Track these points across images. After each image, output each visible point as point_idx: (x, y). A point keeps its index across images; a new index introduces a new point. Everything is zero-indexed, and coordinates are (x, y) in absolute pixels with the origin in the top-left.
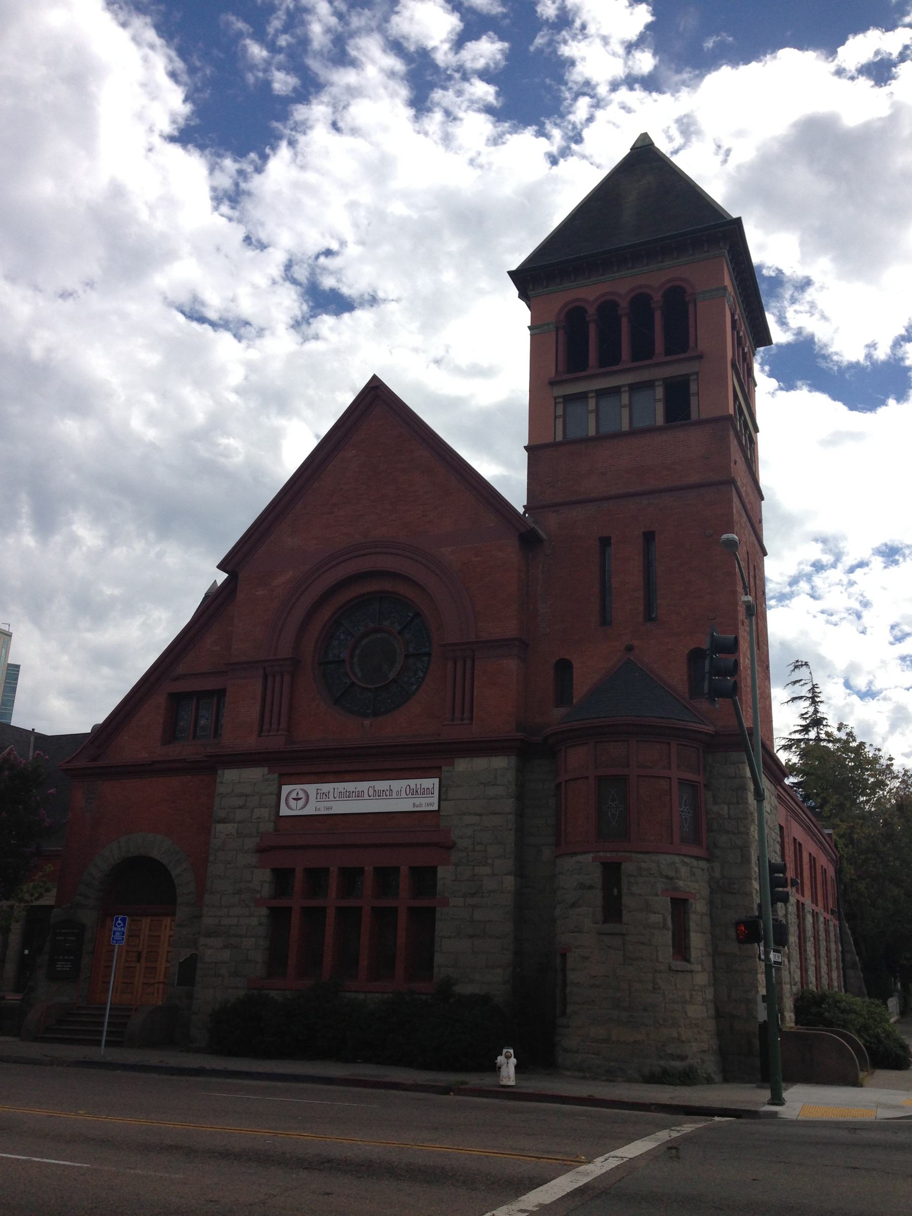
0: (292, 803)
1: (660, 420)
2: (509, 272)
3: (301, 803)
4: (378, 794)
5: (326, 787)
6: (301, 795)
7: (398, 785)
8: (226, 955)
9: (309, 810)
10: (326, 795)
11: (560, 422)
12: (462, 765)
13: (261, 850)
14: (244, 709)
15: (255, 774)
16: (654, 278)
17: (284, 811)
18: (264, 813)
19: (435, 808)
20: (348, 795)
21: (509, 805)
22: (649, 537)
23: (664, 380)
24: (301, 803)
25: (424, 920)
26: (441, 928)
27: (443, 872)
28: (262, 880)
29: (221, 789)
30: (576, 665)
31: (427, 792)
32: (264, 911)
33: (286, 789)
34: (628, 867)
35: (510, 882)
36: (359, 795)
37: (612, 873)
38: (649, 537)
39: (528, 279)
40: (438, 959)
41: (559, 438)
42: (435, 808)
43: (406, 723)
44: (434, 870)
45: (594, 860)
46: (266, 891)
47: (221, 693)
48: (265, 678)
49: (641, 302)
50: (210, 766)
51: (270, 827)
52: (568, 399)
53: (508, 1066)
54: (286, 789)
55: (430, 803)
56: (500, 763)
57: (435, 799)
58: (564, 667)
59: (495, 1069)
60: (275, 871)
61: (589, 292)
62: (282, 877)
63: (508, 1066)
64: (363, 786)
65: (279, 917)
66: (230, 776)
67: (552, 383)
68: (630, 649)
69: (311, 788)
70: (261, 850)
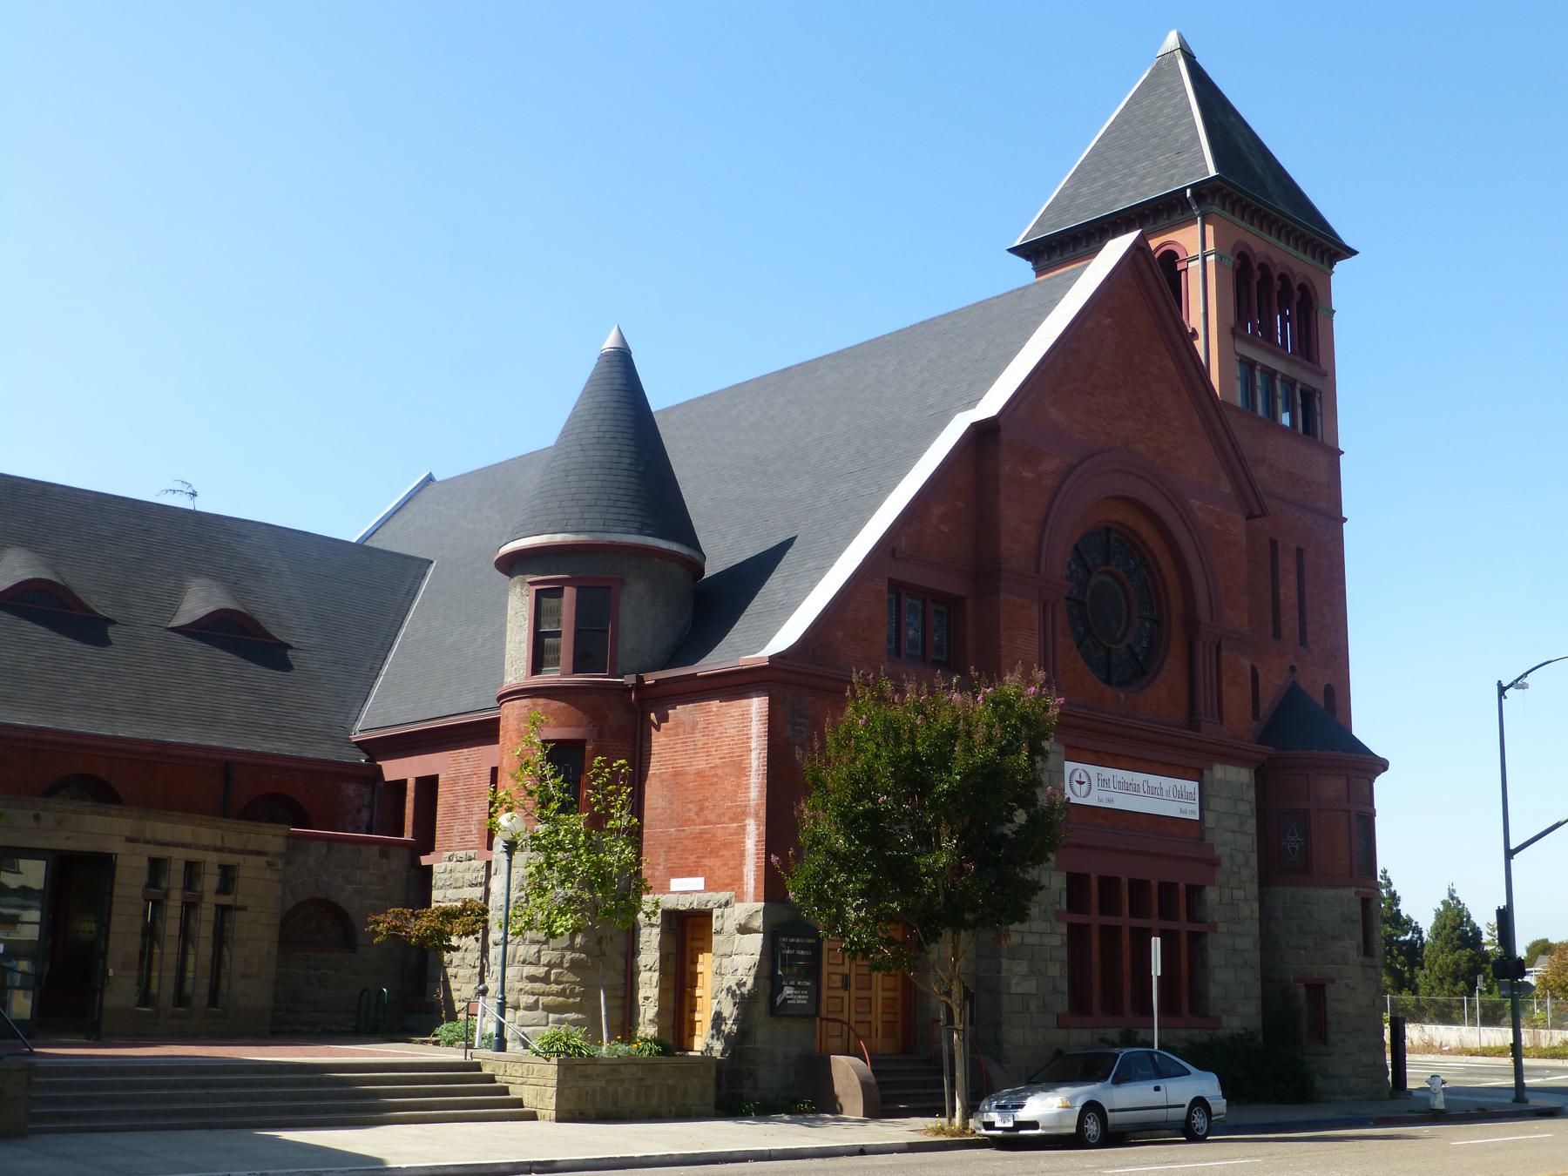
0: (1076, 786)
3: (1085, 787)
4: (1153, 792)
5: (1108, 773)
6: (1084, 779)
7: (1167, 783)
10: (1106, 782)
21: (1251, 825)
24: (1085, 787)
26: (1215, 957)
27: (1211, 894)
31: (1189, 796)
32: (1064, 929)
44: (1201, 888)
45: (1357, 893)
55: (1191, 811)
64: (1139, 778)
65: (1077, 935)
69: (1093, 770)
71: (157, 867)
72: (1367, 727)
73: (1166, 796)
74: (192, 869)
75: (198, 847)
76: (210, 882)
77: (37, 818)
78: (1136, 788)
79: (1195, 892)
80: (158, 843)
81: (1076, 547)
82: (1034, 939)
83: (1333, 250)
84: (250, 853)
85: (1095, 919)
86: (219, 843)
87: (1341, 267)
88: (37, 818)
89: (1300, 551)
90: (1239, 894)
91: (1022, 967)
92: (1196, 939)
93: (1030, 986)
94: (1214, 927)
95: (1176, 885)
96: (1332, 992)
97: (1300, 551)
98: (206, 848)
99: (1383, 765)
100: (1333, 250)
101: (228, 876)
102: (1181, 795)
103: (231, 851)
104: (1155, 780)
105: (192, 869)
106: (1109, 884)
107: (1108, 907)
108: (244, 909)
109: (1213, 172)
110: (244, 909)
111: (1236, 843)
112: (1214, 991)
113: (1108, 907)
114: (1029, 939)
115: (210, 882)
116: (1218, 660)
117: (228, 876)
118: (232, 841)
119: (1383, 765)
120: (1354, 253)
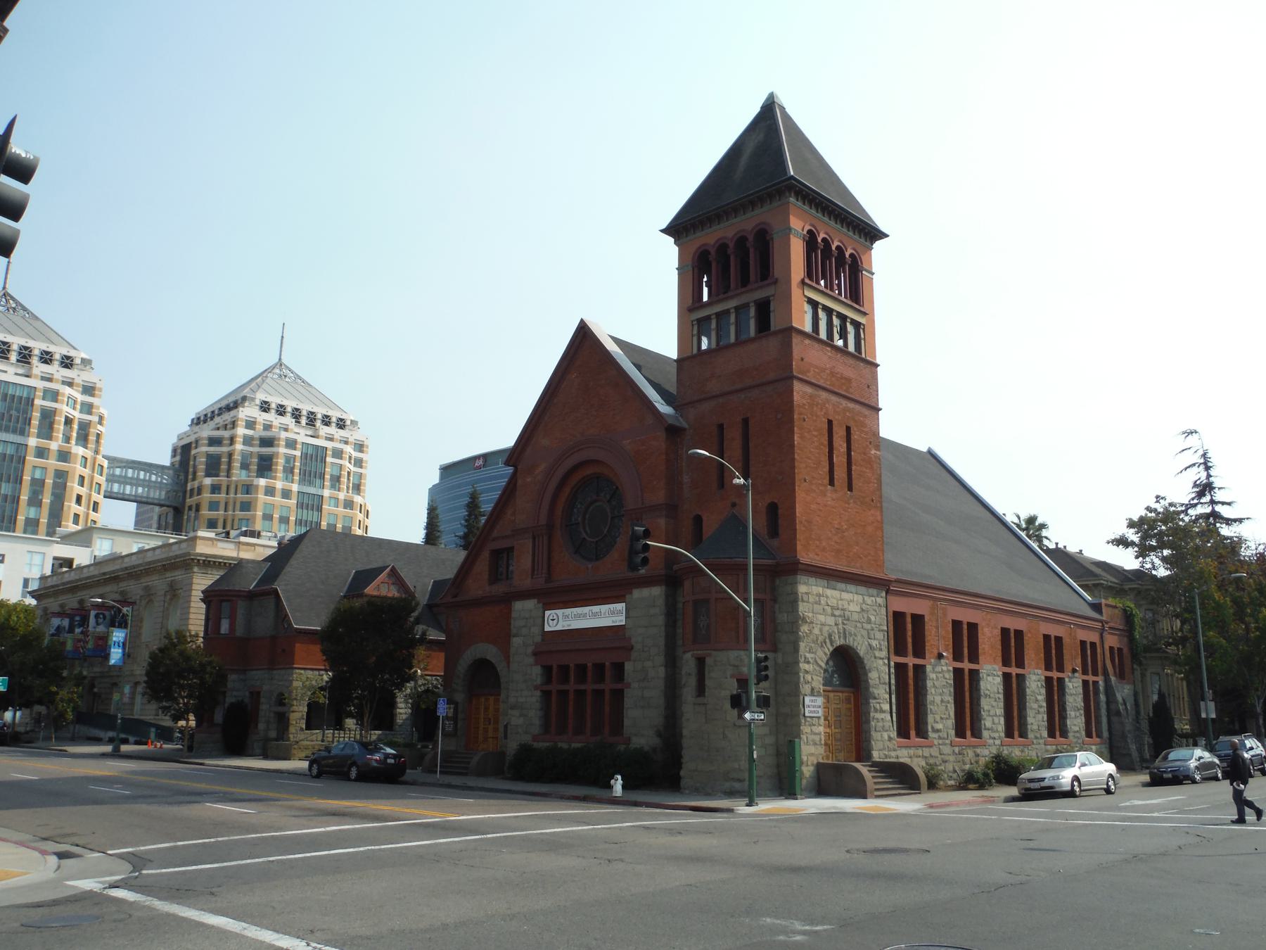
1: (752, 333)
2: (662, 231)
4: (595, 615)
5: (568, 611)
7: (604, 608)
8: (521, 721)
9: (559, 628)
11: (695, 339)
12: (637, 593)
13: (535, 654)
14: (523, 562)
15: (530, 604)
16: (745, 223)
17: (547, 629)
18: (536, 630)
20: (578, 616)
21: (661, 620)
22: (746, 422)
23: (755, 302)
25: (618, 695)
26: (628, 702)
27: (628, 667)
28: (536, 672)
29: (514, 615)
30: (704, 518)
31: (620, 612)
32: (538, 693)
33: (547, 613)
34: (709, 661)
35: (662, 671)
37: (701, 662)
38: (746, 422)
39: (676, 229)
40: (627, 722)
41: (695, 351)
43: (612, 565)
46: (539, 681)
47: (511, 549)
48: (534, 538)
49: (741, 241)
50: (507, 600)
51: (538, 639)
52: (699, 321)
53: (618, 784)
54: (547, 613)
55: (620, 620)
56: (657, 592)
57: (623, 618)
58: (698, 520)
59: (611, 787)
60: (544, 667)
61: (710, 237)
62: (547, 670)
63: (618, 784)
65: (546, 695)
66: (518, 606)
67: (691, 310)
68: (734, 505)
69: (560, 612)
70: (535, 654)
73: (607, 615)
78: (585, 615)
79: (619, 668)
90: (648, 664)
91: (516, 713)
93: (521, 721)
94: (629, 686)
104: (596, 609)
106: (564, 669)
113: (565, 680)
114: (521, 700)
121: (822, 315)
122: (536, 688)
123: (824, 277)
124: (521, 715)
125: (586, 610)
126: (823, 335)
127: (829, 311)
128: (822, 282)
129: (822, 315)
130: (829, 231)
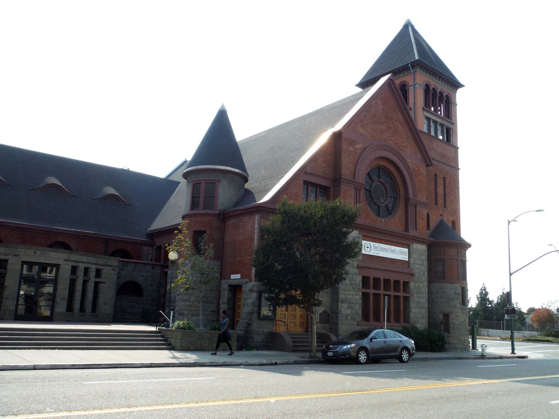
0: (366, 248)
3: (369, 249)
4: (392, 251)
5: (377, 245)
6: (369, 246)
8: (349, 311)
9: (371, 253)
10: (376, 247)
19: (407, 260)
24: (369, 249)
26: (412, 304)
27: (412, 284)
31: (405, 253)
36: (387, 250)
42: (407, 260)
55: (405, 258)
62: (365, 280)
65: (365, 296)
69: (372, 244)
71: (74, 269)
72: (465, 234)
74: (86, 270)
75: (89, 263)
76: (92, 274)
77: (35, 253)
78: (387, 250)
79: (406, 284)
80: (75, 262)
81: (368, 173)
82: (351, 297)
83: (456, 85)
84: (107, 266)
85: (371, 291)
86: (96, 262)
87: (459, 91)
88: (35, 253)
89: (444, 178)
90: (421, 285)
91: (345, 305)
92: (406, 299)
93: (349, 311)
94: (412, 295)
95: (400, 281)
96: (451, 317)
97: (444, 178)
98: (92, 264)
99: (469, 246)
100: (456, 85)
101: (98, 273)
102: (402, 253)
103: (100, 265)
104: (393, 248)
105: (86, 270)
106: (376, 280)
107: (377, 286)
108: (104, 283)
109: (417, 57)
110: (104, 283)
111: (421, 268)
112: (412, 315)
113: (377, 286)
114: (348, 297)
115: (92, 274)
116: (416, 211)
117: (98, 273)
118: (101, 262)
119: (469, 246)
120: (463, 86)
121: (432, 124)
122: (359, 290)
123: (433, 106)
124: (349, 307)
125: (388, 247)
126: (433, 133)
127: (435, 122)
128: (432, 109)
129: (432, 124)
130: (435, 83)
